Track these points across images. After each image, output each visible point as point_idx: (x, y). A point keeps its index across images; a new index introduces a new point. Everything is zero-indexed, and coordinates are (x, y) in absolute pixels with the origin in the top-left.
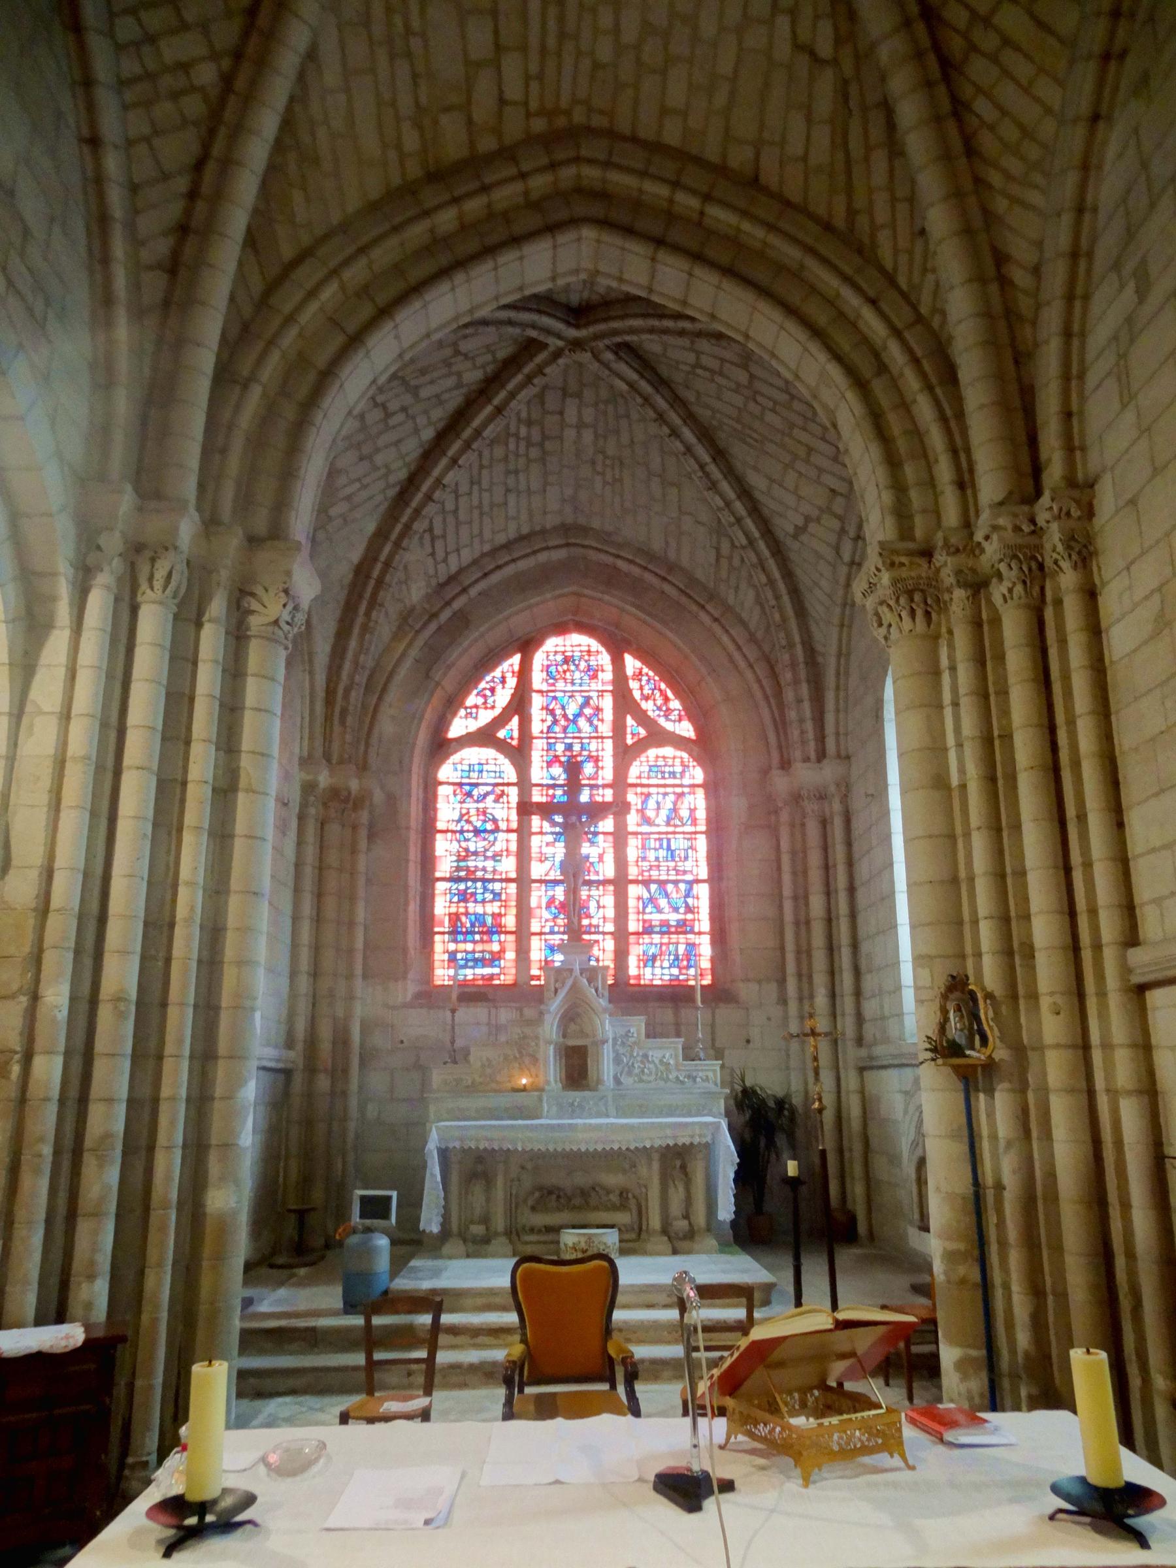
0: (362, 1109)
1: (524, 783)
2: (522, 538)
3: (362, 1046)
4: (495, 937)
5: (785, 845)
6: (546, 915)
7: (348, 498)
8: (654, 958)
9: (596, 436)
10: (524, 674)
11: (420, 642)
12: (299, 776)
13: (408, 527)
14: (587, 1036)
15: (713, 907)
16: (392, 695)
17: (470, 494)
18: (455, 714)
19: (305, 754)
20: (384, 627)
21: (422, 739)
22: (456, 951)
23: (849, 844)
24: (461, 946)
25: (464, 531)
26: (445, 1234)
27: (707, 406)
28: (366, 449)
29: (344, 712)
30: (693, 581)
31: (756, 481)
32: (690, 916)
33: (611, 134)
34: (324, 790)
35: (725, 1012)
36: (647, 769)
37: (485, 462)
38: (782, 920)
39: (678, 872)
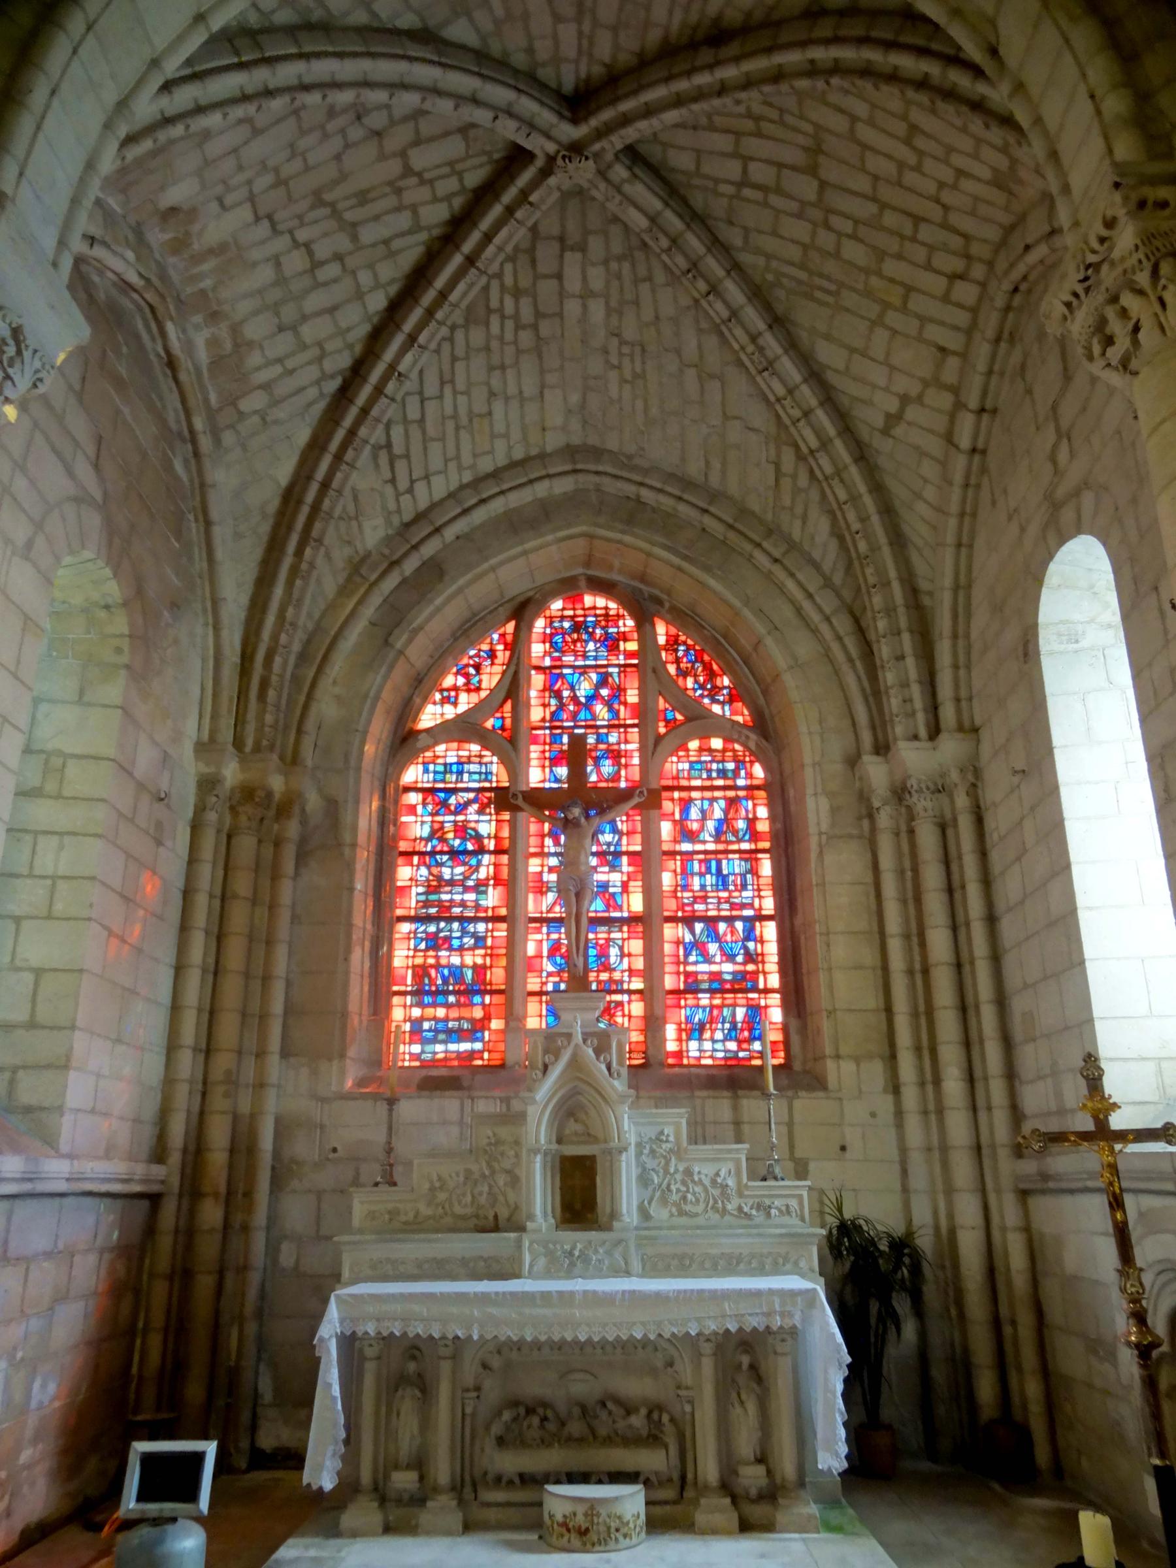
0: (273, 1249)
2: (513, 465)
3: (277, 1154)
4: (477, 999)
5: (887, 861)
6: (549, 967)
7: (266, 387)
8: (701, 1028)
9: (609, 311)
11: (376, 600)
12: (190, 768)
13: (352, 433)
14: (594, 1139)
15: (782, 953)
16: (338, 666)
17: (441, 397)
18: (426, 699)
19: (205, 736)
20: (326, 578)
21: (379, 729)
22: (422, 1019)
23: (983, 854)
24: (430, 1012)
25: (435, 448)
26: (348, 1489)
27: (758, 251)
28: (289, 313)
29: (264, 685)
30: (744, 512)
31: (828, 354)
32: (750, 967)
34: (232, 790)
35: (806, 1104)
36: (686, 766)
37: (460, 351)
38: (885, 968)
39: (734, 907)
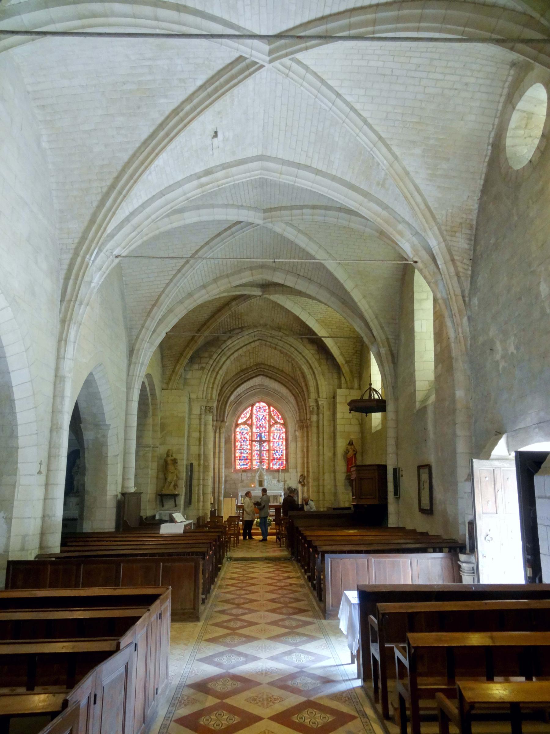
1: (252, 431)
2: (251, 387)
10: (252, 411)
33: (264, 364)
35: (287, 474)
